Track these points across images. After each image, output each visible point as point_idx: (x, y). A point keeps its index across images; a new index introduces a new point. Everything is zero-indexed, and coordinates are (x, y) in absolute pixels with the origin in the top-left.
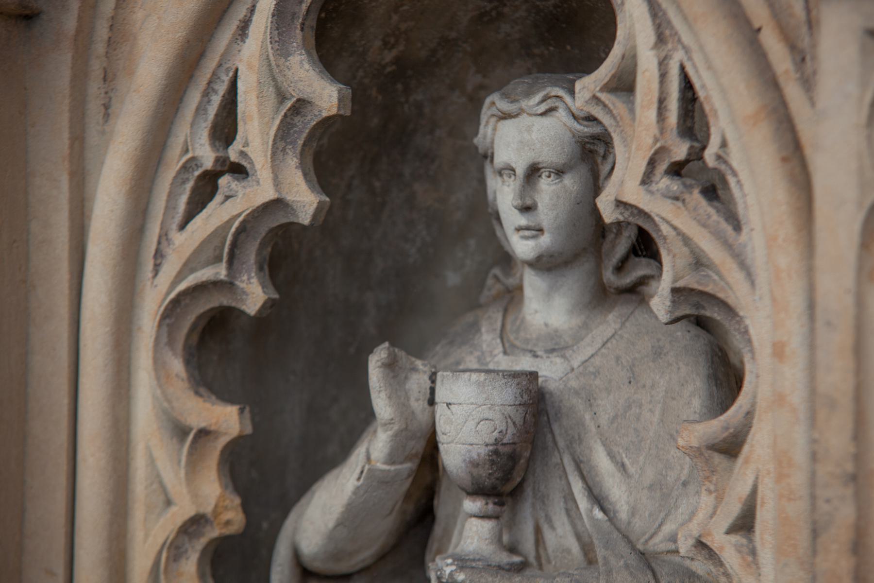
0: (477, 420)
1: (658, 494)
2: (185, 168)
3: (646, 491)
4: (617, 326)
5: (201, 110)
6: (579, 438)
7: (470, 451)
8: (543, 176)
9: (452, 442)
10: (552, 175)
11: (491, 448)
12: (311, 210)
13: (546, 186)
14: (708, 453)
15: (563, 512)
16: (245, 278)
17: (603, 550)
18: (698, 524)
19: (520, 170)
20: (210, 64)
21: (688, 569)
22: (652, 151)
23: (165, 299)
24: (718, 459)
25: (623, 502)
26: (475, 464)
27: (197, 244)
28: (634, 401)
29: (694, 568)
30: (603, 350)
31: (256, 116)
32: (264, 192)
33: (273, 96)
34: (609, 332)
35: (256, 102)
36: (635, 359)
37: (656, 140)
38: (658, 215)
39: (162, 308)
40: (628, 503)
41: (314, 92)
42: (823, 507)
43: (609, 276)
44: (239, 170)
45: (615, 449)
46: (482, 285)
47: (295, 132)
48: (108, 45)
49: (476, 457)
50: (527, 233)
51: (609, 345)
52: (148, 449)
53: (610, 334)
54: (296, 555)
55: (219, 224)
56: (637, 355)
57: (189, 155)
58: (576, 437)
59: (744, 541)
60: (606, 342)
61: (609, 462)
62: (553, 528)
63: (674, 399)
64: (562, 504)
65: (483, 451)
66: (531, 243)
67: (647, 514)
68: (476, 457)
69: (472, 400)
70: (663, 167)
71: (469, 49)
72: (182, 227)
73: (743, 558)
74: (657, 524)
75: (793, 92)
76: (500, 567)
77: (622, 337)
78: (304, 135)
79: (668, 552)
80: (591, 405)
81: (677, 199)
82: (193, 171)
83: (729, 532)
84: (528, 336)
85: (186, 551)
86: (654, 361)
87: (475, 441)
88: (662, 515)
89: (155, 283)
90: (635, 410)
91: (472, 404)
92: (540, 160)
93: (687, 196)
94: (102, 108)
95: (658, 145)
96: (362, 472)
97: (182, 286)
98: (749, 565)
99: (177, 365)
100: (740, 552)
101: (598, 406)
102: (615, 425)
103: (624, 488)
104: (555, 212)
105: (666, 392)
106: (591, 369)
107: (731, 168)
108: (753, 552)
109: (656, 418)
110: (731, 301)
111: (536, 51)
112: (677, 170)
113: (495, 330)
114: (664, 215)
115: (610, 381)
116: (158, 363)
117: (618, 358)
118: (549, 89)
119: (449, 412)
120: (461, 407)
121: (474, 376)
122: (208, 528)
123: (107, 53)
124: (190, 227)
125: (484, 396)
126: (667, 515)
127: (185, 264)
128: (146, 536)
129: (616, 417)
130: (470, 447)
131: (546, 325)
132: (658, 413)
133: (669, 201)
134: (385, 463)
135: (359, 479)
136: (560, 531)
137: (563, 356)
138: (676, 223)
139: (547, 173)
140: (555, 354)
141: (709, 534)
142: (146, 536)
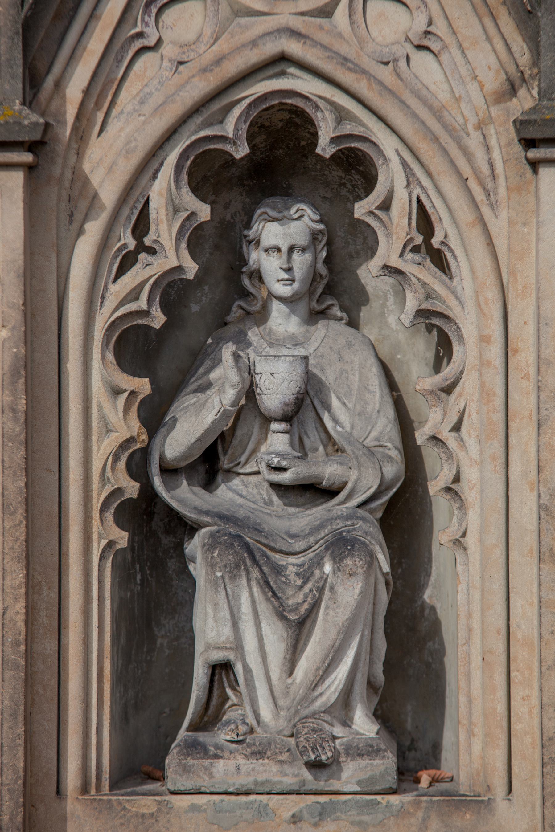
0: (289, 381)
1: (363, 418)
2: (119, 250)
3: (357, 416)
4: (325, 331)
5: (129, 218)
6: (320, 390)
7: (285, 398)
8: (295, 252)
9: (274, 393)
10: (300, 251)
11: (295, 396)
12: (194, 272)
13: (296, 256)
14: (438, 393)
15: (314, 429)
16: (154, 309)
17: (350, 447)
18: (429, 429)
19: (284, 249)
20: (136, 193)
21: (387, 454)
22: (406, 240)
23: (107, 321)
24: (443, 395)
25: (347, 423)
26: (286, 405)
27: (128, 291)
28: (344, 370)
29: (390, 454)
30: (322, 344)
31: (165, 221)
32: (173, 262)
33: (172, 210)
34: (322, 335)
35: (165, 214)
36: (339, 348)
37: (408, 234)
38: (409, 272)
39: (106, 326)
40: (350, 423)
41: (197, 208)
42: (544, 412)
43: (314, 304)
44: (152, 251)
45: (340, 395)
46: (228, 311)
47: (185, 230)
48: (72, 183)
49: (287, 400)
50: (288, 282)
51: (324, 341)
52: (99, 403)
53: (323, 335)
54: (162, 457)
55: (142, 280)
56: (340, 346)
57: (122, 242)
58: (318, 390)
59: (457, 435)
60: (323, 340)
61: (338, 402)
62: (309, 438)
63: (363, 368)
64: (314, 425)
65: (292, 397)
66: (289, 288)
67: (359, 427)
68: (287, 400)
69: (287, 371)
70: (410, 247)
71: (212, 182)
72: (115, 281)
73: (459, 443)
74: (367, 433)
75: (486, 210)
76: (298, 457)
77: (329, 337)
78: (190, 231)
79: (375, 446)
80: (324, 373)
81: (420, 264)
82: (122, 251)
83: (450, 431)
84: (278, 338)
85: (120, 457)
86: (349, 349)
87: (288, 392)
88: (369, 428)
89: (101, 312)
90: (345, 375)
91: (287, 373)
92: (296, 243)
93: (424, 263)
94: (68, 217)
95: (409, 237)
96: (219, 411)
97: (118, 313)
98: (462, 447)
99: (110, 357)
100: (457, 440)
101: (327, 373)
102: (337, 383)
103: (347, 415)
104: (302, 271)
105: (359, 365)
106: (319, 354)
107: (449, 248)
108: (462, 440)
109: (357, 379)
110: (451, 315)
111: (246, 183)
112: (416, 249)
113: (257, 335)
114: (413, 272)
115: (330, 360)
116: (103, 357)
117: (331, 348)
118: (298, 205)
119: (272, 378)
120: (280, 375)
121: (287, 358)
122: (134, 444)
123: (71, 187)
124: (119, 281)
125: (293, 368)
126: (372, 428)
127: (120, 302)
128: (99, 449)
129: (336, 378)
130: (285, 396)
131: (286, 331)
132: (357, 376)
133: (416, 265)
134: (230, 406)
135: (216, 415)
136: (312, 439)
137: (304, 347)
138: (419, 276)
139: (298, 251)
140: (298, 347)
141: (440, 432)
142: (99, 449)
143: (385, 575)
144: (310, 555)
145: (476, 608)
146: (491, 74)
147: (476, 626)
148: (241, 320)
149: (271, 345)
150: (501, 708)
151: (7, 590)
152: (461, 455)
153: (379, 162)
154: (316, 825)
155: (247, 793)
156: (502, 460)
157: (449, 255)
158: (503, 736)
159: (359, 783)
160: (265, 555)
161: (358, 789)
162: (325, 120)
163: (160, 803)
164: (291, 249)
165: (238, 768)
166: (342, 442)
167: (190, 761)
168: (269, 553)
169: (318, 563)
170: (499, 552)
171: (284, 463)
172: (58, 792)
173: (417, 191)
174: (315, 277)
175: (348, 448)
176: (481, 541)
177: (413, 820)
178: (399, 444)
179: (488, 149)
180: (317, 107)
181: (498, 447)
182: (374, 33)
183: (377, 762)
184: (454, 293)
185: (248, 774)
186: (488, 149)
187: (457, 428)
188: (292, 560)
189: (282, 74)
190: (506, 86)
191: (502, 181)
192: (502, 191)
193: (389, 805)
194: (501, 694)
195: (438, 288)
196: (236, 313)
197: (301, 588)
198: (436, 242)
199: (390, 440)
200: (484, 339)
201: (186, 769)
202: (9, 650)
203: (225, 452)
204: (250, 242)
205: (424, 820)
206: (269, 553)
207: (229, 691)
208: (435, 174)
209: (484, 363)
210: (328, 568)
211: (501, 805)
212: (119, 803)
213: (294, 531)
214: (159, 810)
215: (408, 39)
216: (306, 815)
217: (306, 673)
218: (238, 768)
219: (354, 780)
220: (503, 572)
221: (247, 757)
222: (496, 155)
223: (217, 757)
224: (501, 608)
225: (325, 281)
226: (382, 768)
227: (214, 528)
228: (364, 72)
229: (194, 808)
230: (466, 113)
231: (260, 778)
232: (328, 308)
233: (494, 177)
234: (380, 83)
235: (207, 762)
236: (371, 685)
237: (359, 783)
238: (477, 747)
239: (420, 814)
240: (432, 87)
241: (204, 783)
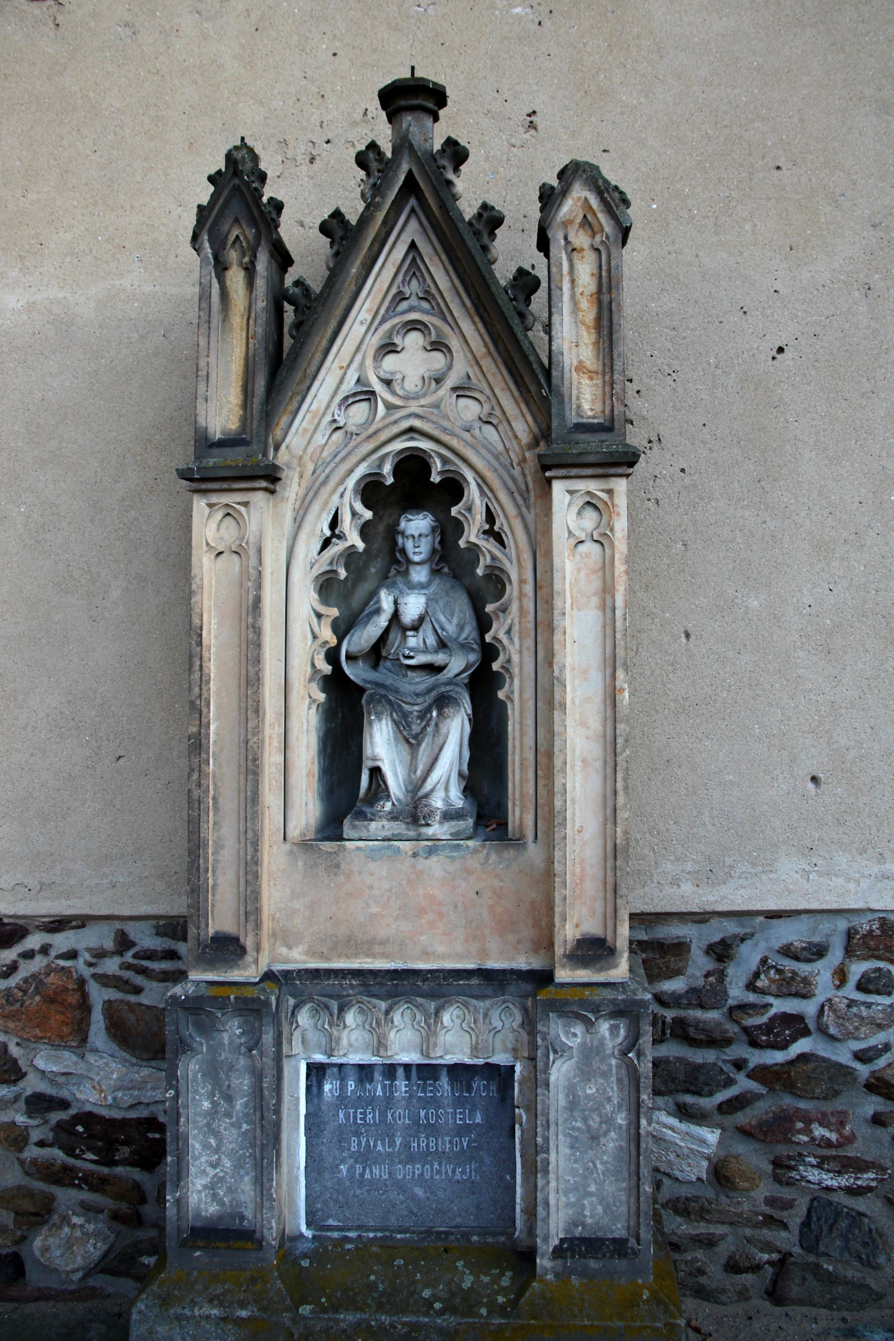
26: (414, 621)
65: (417, 617)
108: (511, 639)
112: (485, 532)
138: (488, 547)
143: (468, 715)
144: (426, 704)
145: (517, 734)
146: (526, 434)
147: (517, 743)
148: (395, 576)
149: (409, 588)
150: (531, 791)
151: (249, 729)
152: (510, 647)
153: (465, 485)
154: (427, 858)
155: (389, 840)
156: (533, 650)
157: (503, 535)
158: (532, 807)
159: (451, 834)
160: (400, 706)
161: (449, 837)
162: (435, 462)
163: (339, 846)
164: (420, 535)
165: (383, 826)
166: (446, 641)
167: (357, 823)
168: (403, 704)
169: (428, 710)
170: (531, 703)
171: (412, 654)
172: (285, 839)
173: (486, 500)
174: (434, 551)
175: (449, 644)
176: (521, 696)
177: (481, 855)
178: (479, 641)
179: (524, 476)
180: (431, 456)
181: (530, 642)
182: (463, 416)
183: (460, 823)
184: (506, 555)
185: (389, 830)
186: (524, 476)
187: (509, 632)
188: (416, 708)
189: (412, 439)
190: (533, 441)
191: (532, 493)
192: (532, 499)
193: (467, 847)
194: (532, 783)
195: (498, 553)
196: (393, 572)
197: (419, 724)
198: (496, 528)
199: (473, 639)
200: (522, 581)
201: (354, 827)
202: (250, 763)
203: (384, 647)
204: (399, 533)
205: (487, 854)
206: (403, 704)
207: (381, 783)
208: (495, 490)
209: (521, 595)
210: (435, 714)
211: (531, 846)
212: (317, 845)
213: (417, 691)
214: (339, 850)
215: (480, 419)
216: (421, 853)
217: (422, 772)
218: (383, 826)
219: (448, 833)
220: (533, 714)
221: (388, 820)
222: (529, 479)
223: (372, 820)
224: (531, 734)
225: (440, 554)
226: (464, 826)
227: (373, 691)
228: (455, 435)
229: (358, 848)
230: (512, 457)
231: (396, 832)
232: (442, 568)
233: (528, 490)
234: (465, 441)
235: (366, 823)
236: (460, 774)
237: (451, 834)
238: (517, 813)
239: (485, 851)
240: (494, 444)
241: (364, 834)
